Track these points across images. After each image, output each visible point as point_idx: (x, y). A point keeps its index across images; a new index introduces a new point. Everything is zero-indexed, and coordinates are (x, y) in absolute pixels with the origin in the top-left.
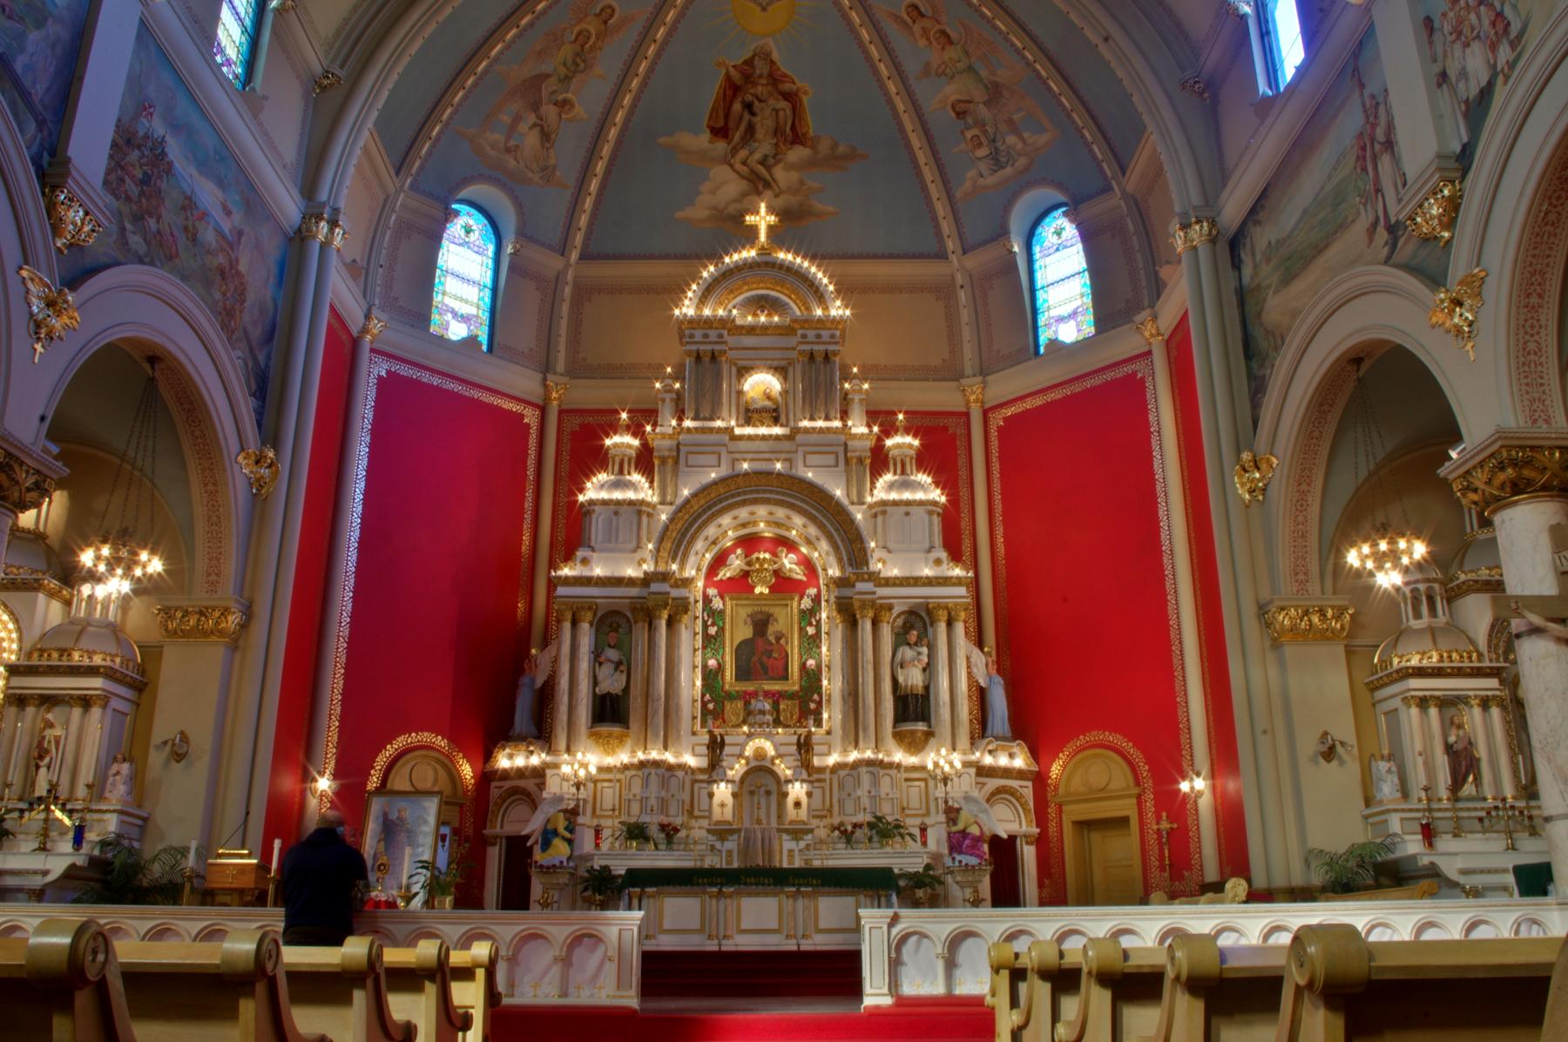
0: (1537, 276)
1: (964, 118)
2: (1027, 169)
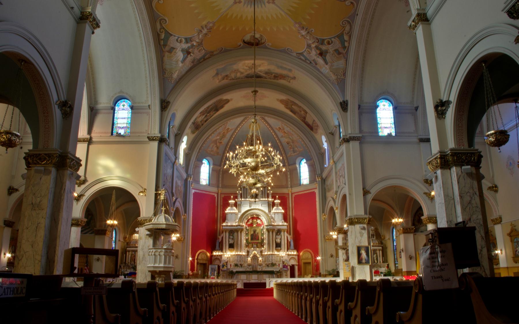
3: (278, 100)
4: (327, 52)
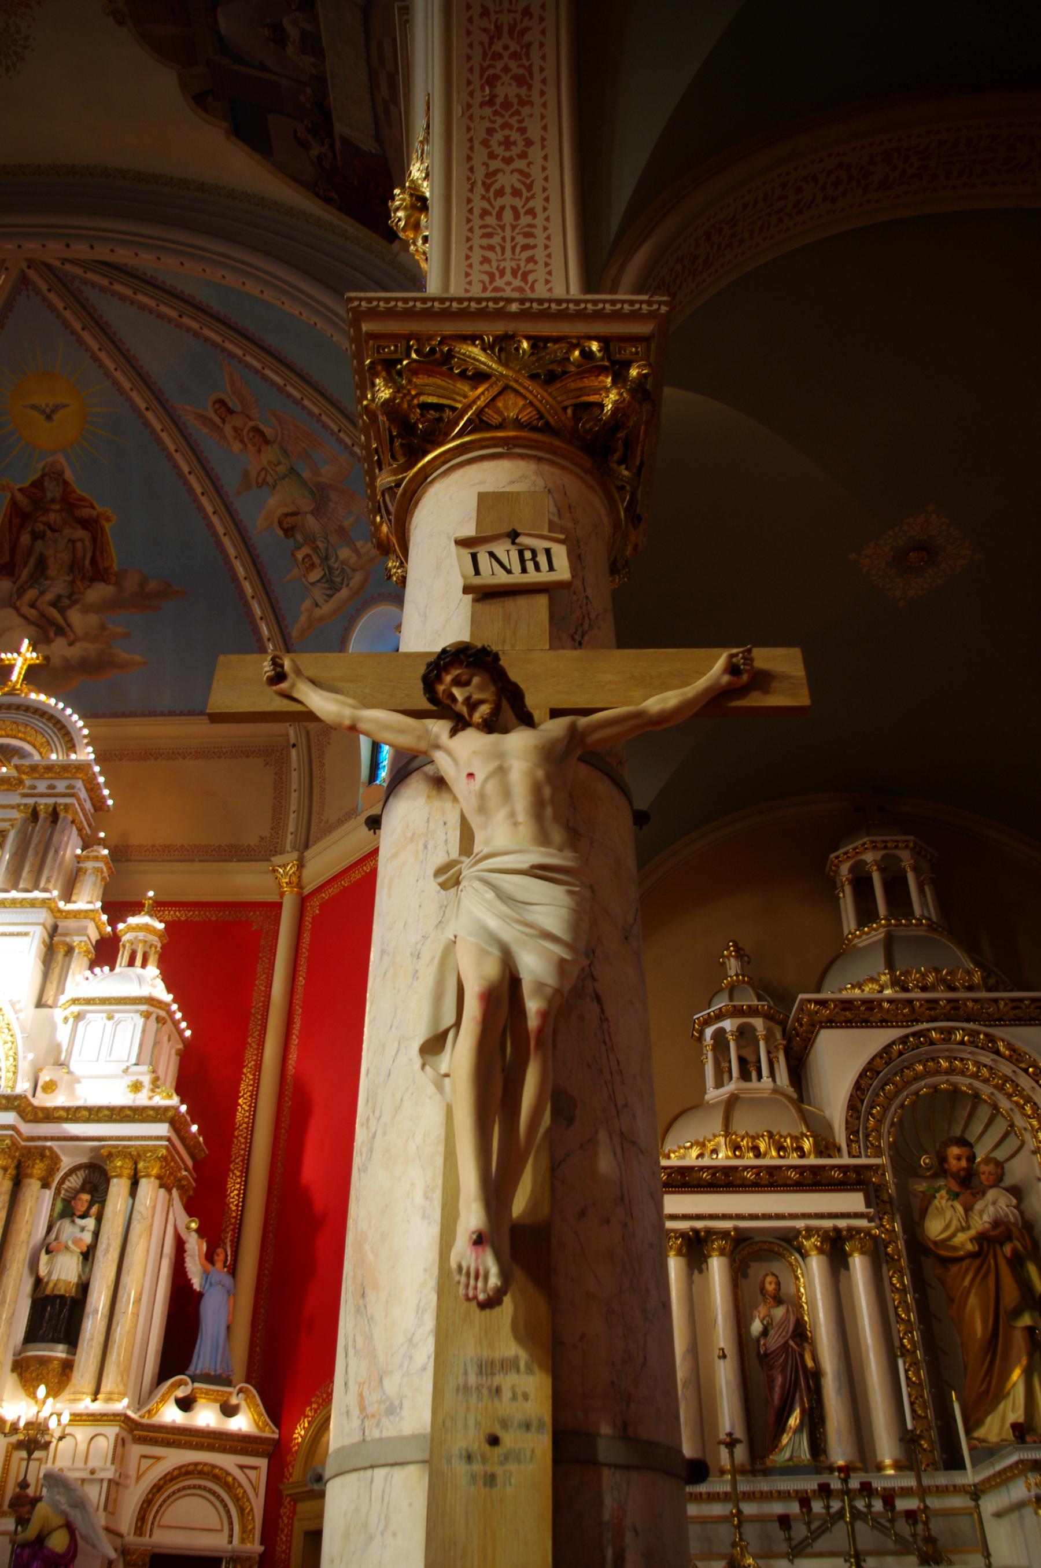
0: (506, 39)
1: (293, 536)
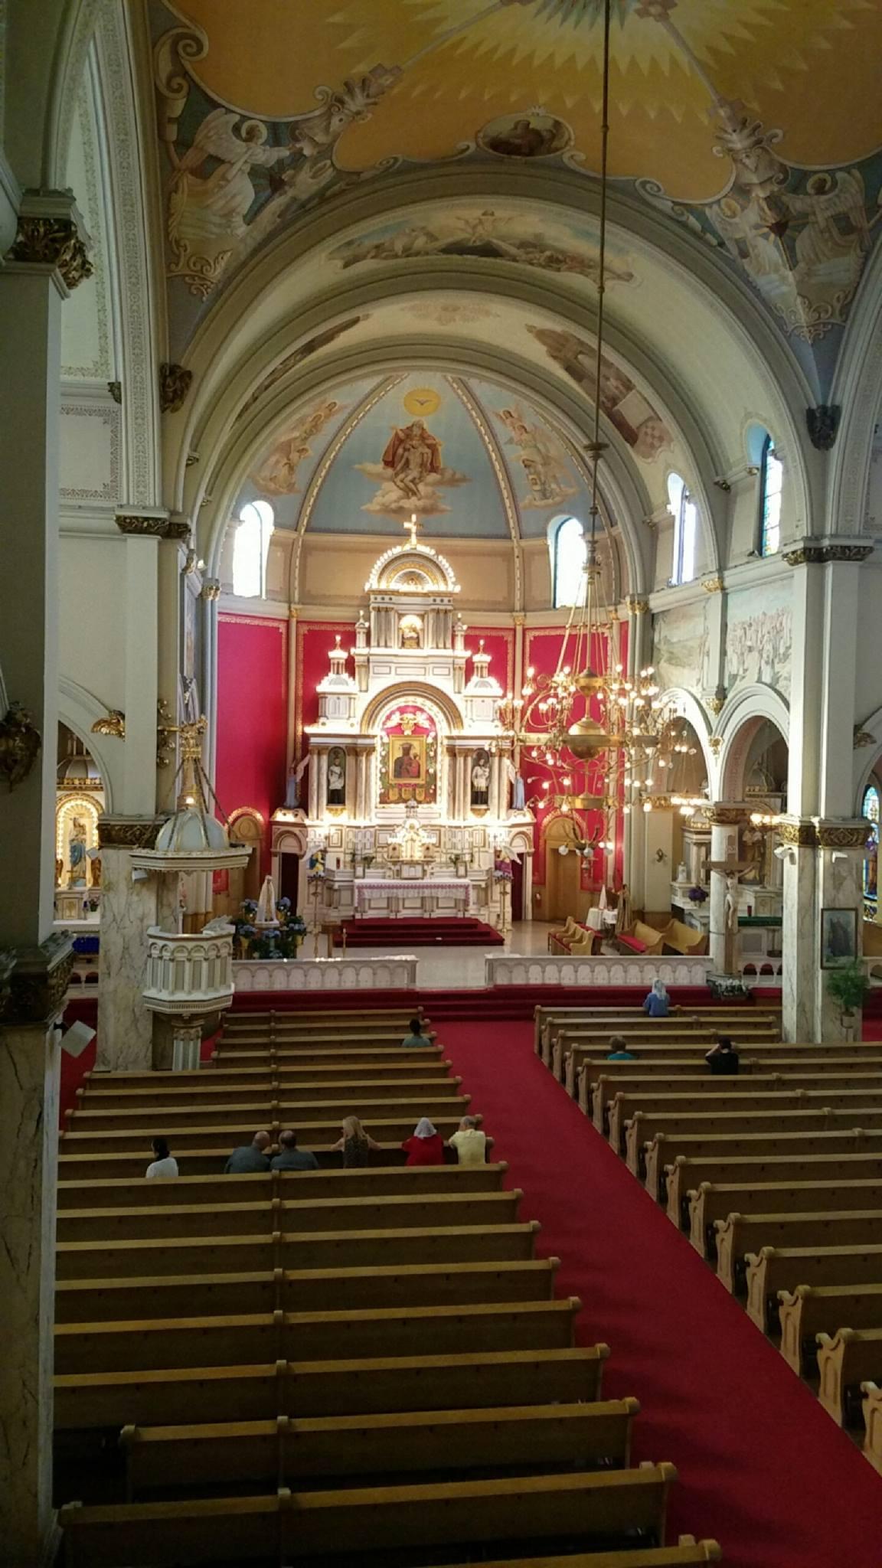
2: (561, 502)
3: (530, 329)
4: (804, 220)
